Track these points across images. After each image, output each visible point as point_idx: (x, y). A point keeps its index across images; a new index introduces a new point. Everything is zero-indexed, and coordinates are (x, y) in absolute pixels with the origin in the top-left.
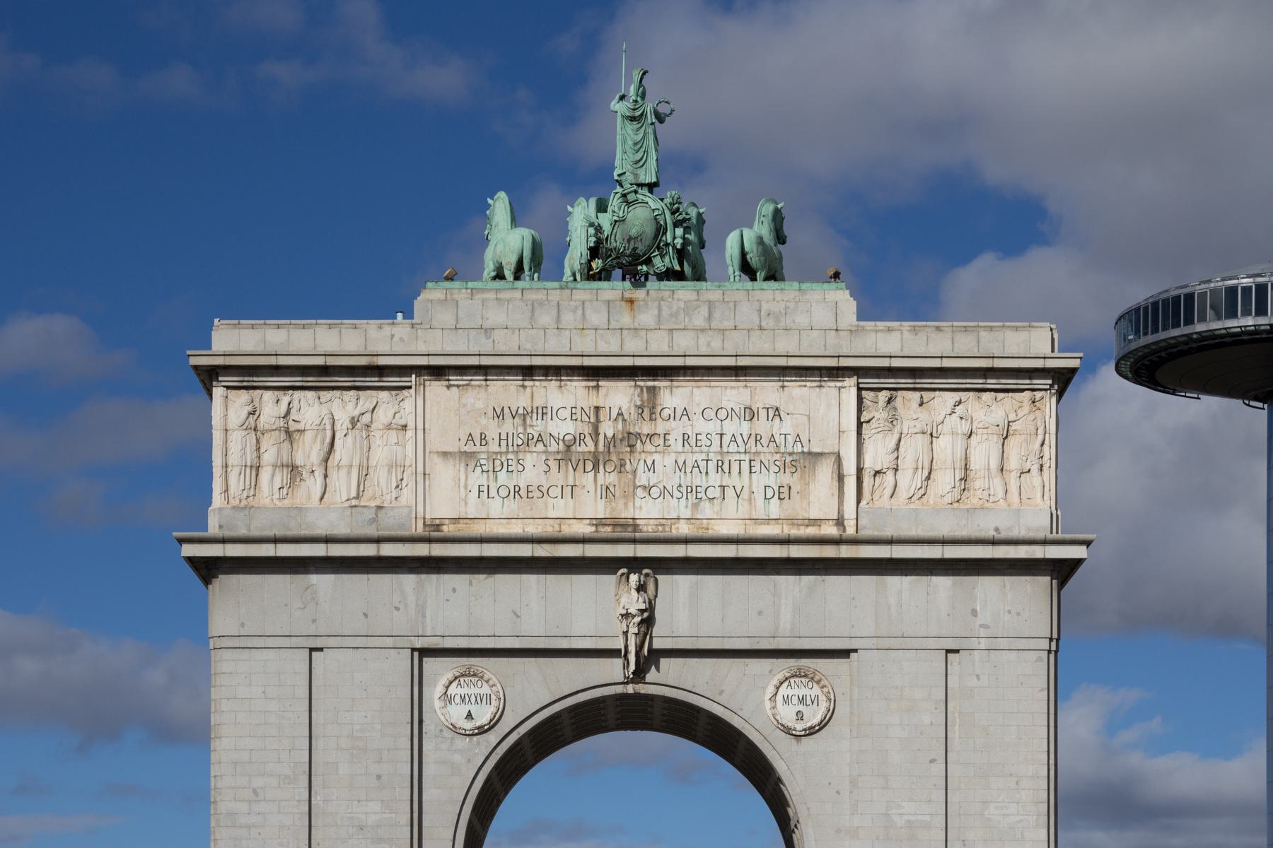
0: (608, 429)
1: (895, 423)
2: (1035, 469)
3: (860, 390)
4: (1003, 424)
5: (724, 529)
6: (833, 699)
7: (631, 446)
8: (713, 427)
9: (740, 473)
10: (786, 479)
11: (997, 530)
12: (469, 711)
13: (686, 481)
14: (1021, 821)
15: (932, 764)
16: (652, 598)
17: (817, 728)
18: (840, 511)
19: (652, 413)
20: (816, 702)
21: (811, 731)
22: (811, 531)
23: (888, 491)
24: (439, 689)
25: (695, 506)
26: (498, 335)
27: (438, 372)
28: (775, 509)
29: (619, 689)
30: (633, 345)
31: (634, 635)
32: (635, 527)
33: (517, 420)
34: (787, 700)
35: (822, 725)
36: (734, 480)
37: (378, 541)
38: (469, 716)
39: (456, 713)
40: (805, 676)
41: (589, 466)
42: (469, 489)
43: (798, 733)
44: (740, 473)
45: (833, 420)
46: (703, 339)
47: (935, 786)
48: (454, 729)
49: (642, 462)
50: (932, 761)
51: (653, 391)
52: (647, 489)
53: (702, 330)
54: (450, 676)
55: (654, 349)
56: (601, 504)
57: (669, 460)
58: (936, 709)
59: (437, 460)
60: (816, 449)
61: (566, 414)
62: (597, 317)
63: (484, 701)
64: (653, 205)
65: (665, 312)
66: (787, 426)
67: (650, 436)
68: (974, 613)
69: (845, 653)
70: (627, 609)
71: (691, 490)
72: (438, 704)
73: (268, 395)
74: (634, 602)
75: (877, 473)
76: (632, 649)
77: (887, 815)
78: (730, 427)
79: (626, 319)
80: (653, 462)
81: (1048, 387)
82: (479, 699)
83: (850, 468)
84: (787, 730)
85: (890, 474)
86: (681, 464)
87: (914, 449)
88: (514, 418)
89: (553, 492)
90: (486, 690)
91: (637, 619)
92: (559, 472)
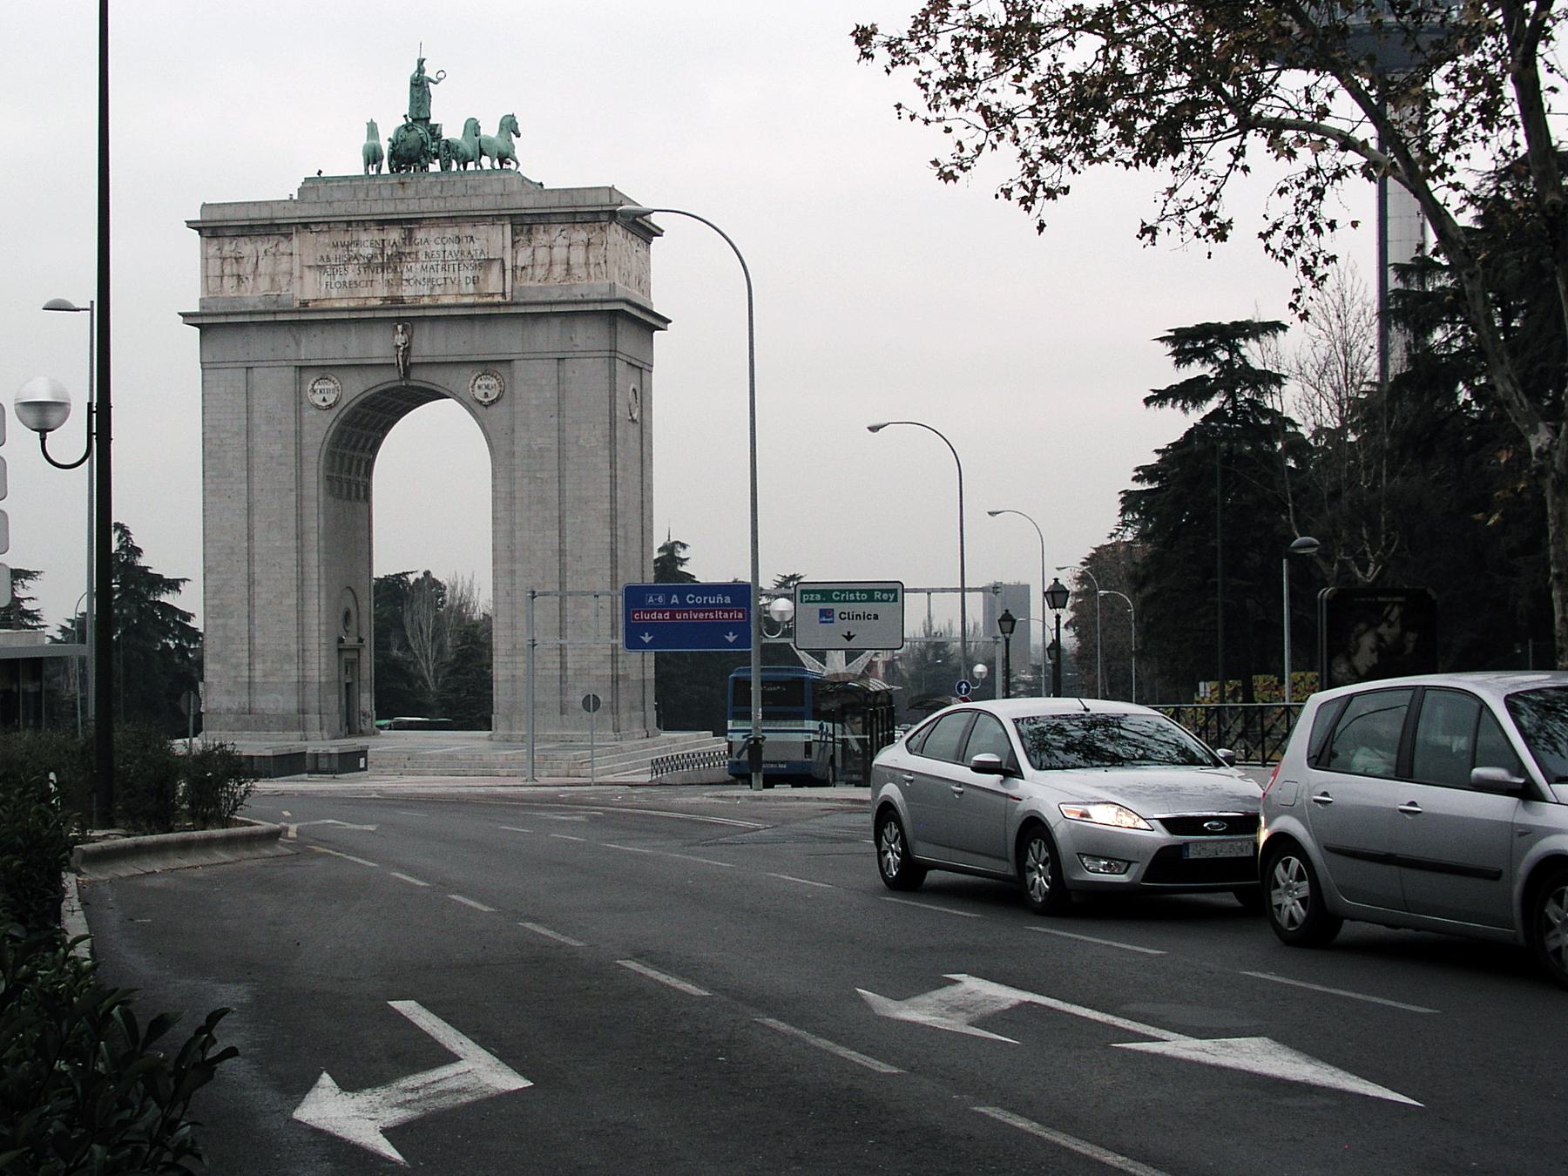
0: (389, 251)
2: (602, 262)
3: (512, 225)
4: (586, 240)
5: (446, 300)
7: (401, 259)
8: (440, 247)
10: (477, 273)
11: (582, 295)
13: (427, 276)
18: (504, 289)
19: (410, 242)
21: (492, 402)
22: (489, 299)
23: (529, 277)
24: (310, 387)
25: (432, 288)
26: (335, 205)
27: (306, 225)
28: (471, 288)
29: (398, 384)
30: (402, 207)
32: (403, 301)
34: (479, 387)
35: (498, 399)
36: (451, 275)
37: (275, 313)
38: (324, 400)
39: (317, 399)
41: (380, 270)
46: (435, 203)
48: (318, 407)
49: (405, 269)
51: (410, 230)
52: (407, 280)
53: (436, 198)
54: (315, 379)
55: (411, 208)
56: (386, 288)
57: (419, 266)
59: (306, 269)
61: (368, 244)
62: (386, 193)
64: (420, 131)
65: (420, 190)
67: (409, 254)
69: (510, 361)
71: (430, 280)
72: (309, 394)
73: (227, 240)
74: (400, 339)
75: (523, 268)
76: (401, 363)
77: (529, 445)
78: (448, 248)
79: (400, 194)
82: (328, 391)
83: (508, 266)
84: (481, 402)
85: (530, 268)
87: (542, 254)
89: (363, 284)
90: (331, 386)
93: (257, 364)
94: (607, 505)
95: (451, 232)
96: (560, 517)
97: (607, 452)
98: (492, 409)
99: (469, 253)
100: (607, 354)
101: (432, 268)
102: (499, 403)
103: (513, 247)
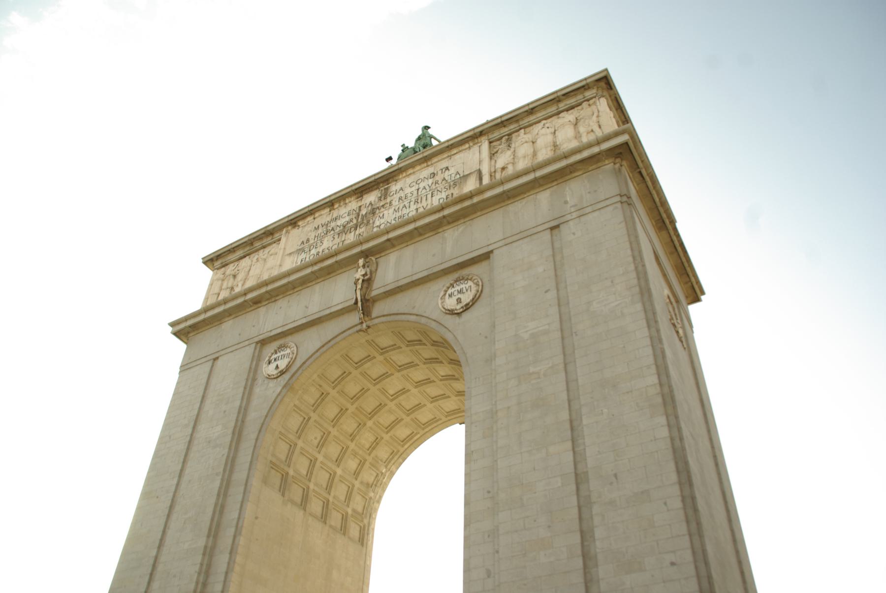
1: (510, 145)
6: (480, 284)
12: (277, 365)
14: (616, 306)
16: (373, 269)
17: (471, 304)
20: (469, 290)
21: (467, 307)
31: (359, 290)
33: (324, 227)
35: (475, 300)
43: (458, 311)
50: (546, 292)
63: (285, 357)
66: (452, 171)
67: (383, 206)
68: (566, 202)
69: (486, 256)
80: (383, 215)
81: (595, 95)
84: (451, 312)
86: (396, 209)
88: (323, 226)
91: (360, 281)
93: (222, 352)
94: (654, 379)
95: (426, 172)
96: (571, 421)
97: (639, 307)
98: (466, 316)
99: (444, 179)
100: (618, 199)
101: (405, 206)
103: (491, 159)
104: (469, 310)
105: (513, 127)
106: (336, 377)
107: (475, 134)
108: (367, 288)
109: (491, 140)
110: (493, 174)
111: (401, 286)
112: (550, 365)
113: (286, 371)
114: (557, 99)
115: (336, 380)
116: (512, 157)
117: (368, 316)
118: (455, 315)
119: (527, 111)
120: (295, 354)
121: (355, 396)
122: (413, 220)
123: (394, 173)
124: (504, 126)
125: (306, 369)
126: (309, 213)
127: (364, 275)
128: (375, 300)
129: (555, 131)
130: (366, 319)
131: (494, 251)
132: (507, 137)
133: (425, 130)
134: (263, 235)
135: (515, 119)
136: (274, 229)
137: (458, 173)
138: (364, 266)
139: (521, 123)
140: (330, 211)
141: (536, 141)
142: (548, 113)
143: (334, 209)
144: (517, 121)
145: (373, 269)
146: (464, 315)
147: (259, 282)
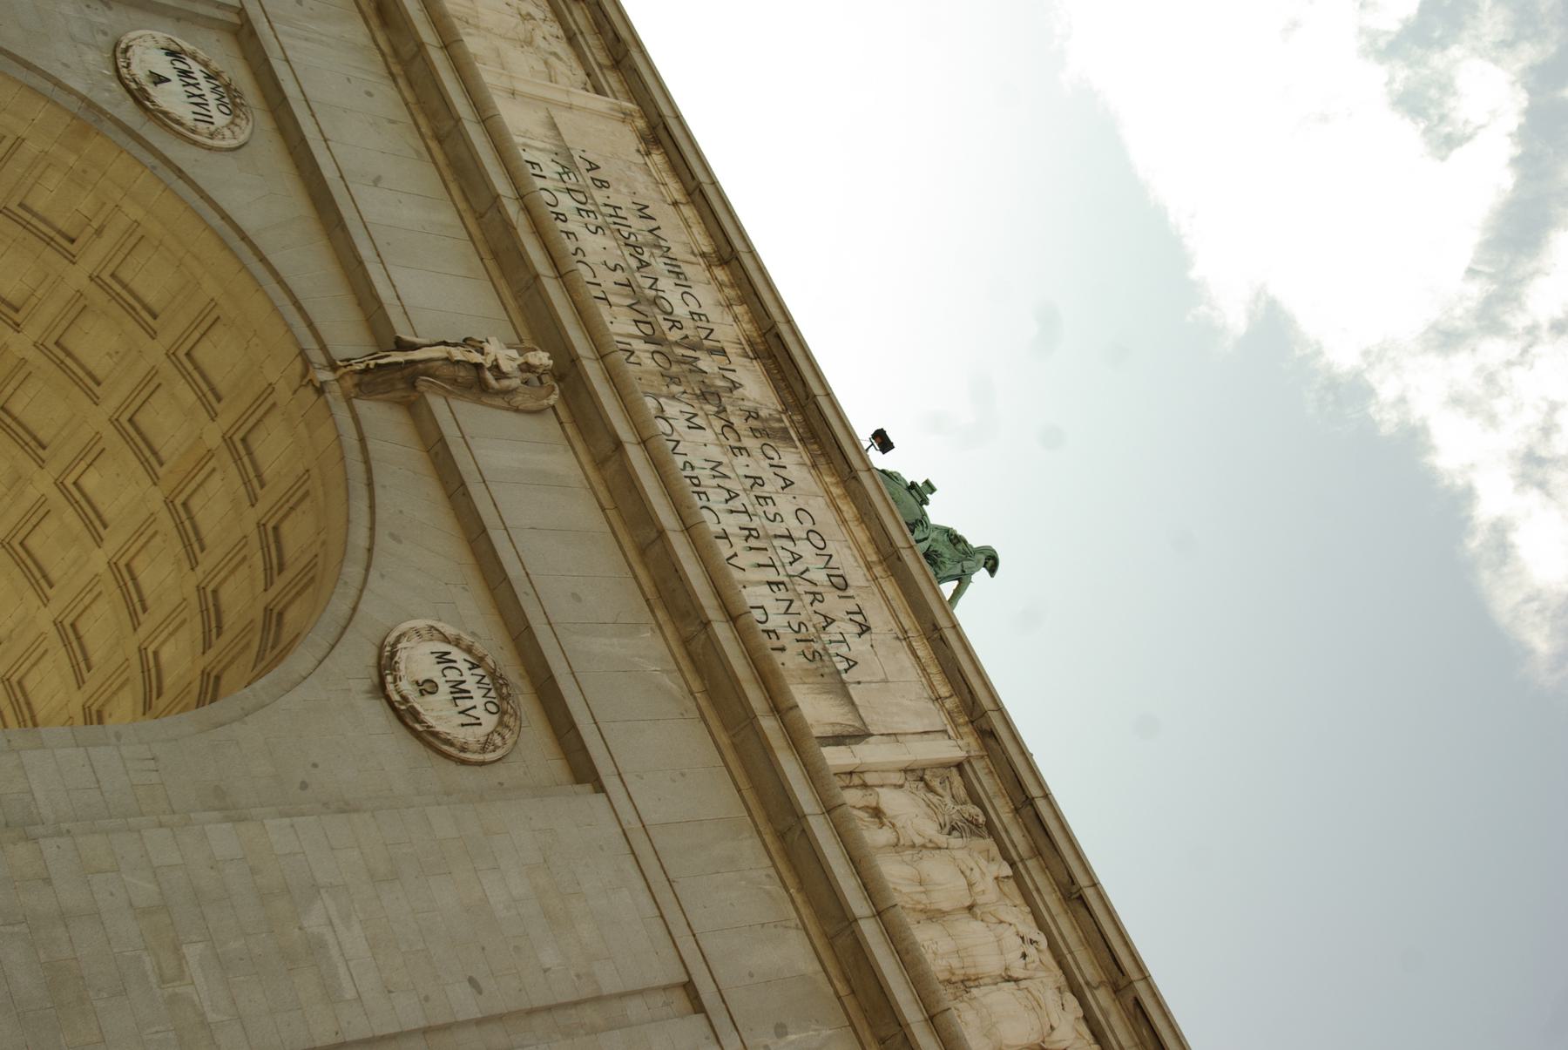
1: (955, 833)
6: (489, 757)
9: (759, 565)
12: (168, 80)
15: (467, 984)
16: (518, 400)
17: (418, 727)
20: (466, 720)
21: (406, 716)
31: (445, 355)
33: (650, 237)
35: (430, 740)
40: (502, 697)
42: (527, 149)
43: (390, 687)
44: (759, 565)
45: (904, 723)
47: (427, 999)
58: (578, 976)
60: (854, 691)
63: (197, 109)
66: (859, 647)
67: (730, 425)
68: (781, 1030)
69: (583, 771)
70: (488, 341)
80: (700, 428)
84: (386, 664)
88: (651, 231)
91: (476, 357)
92: (615, 283)
95: (848, 561)
98: (377, 713)
99: (829, 621)
101: (733, 496)
102: (415, 747)
104: (396, 722)
105: (1017, 837)
106: (136, 285)
107: (984, 714)
108: (454, 381)
109: (967, 767)
110: (856, 780)
111: (466, 494)
112: (212, 1017)
113: (146, 109)
114: (1122, 983)
115: (125, 286)
116: (918, 841)
117: (357, 385)
118: (376, 679)
119: (1073, 881)
120: (209, 142)
121: (69, 354)
122: (689, 522)
123: (839, 456)
124: (1016, 810)
125: (161, 180)
126: (692, 185)
127: (496, 367)
128: (414, 409)
129: (1016, 980)
130: (349, 382)
131: (601, 796)
132: (981, 819)
133: (982, 558)
134: (611, 35)
135: (1042, 842)
136: (636, 71)
137: (852, 664)
138: (527, 367)
139: (1031, 864)
140: (703, 255)
141: (975, 917)
142: (1071, 952)
143: (709, 267)
144: (1037, 852)
145: (518, 400)
146: (380, 706)
147: (456, 21)
